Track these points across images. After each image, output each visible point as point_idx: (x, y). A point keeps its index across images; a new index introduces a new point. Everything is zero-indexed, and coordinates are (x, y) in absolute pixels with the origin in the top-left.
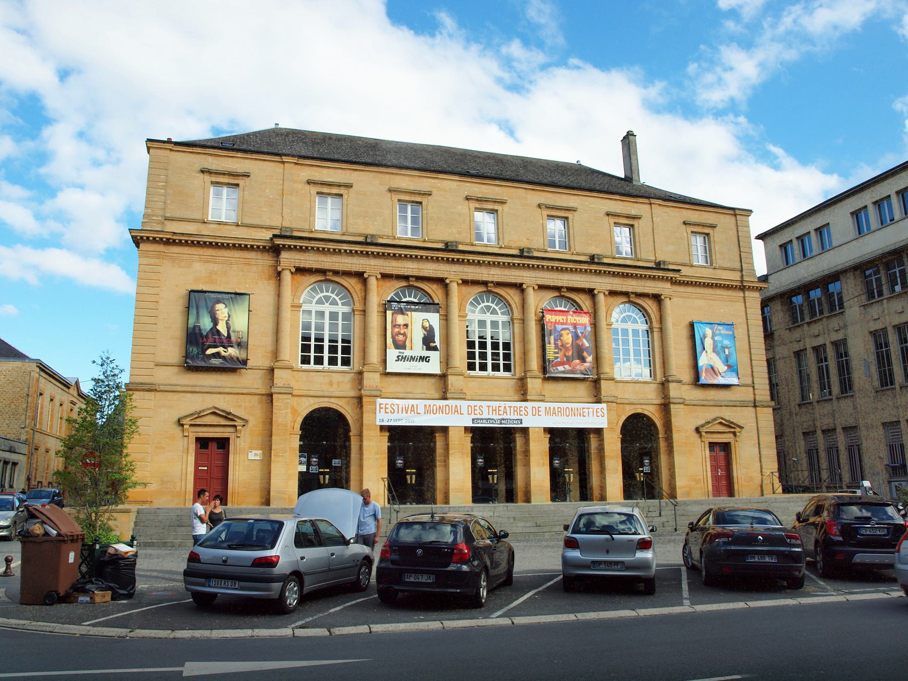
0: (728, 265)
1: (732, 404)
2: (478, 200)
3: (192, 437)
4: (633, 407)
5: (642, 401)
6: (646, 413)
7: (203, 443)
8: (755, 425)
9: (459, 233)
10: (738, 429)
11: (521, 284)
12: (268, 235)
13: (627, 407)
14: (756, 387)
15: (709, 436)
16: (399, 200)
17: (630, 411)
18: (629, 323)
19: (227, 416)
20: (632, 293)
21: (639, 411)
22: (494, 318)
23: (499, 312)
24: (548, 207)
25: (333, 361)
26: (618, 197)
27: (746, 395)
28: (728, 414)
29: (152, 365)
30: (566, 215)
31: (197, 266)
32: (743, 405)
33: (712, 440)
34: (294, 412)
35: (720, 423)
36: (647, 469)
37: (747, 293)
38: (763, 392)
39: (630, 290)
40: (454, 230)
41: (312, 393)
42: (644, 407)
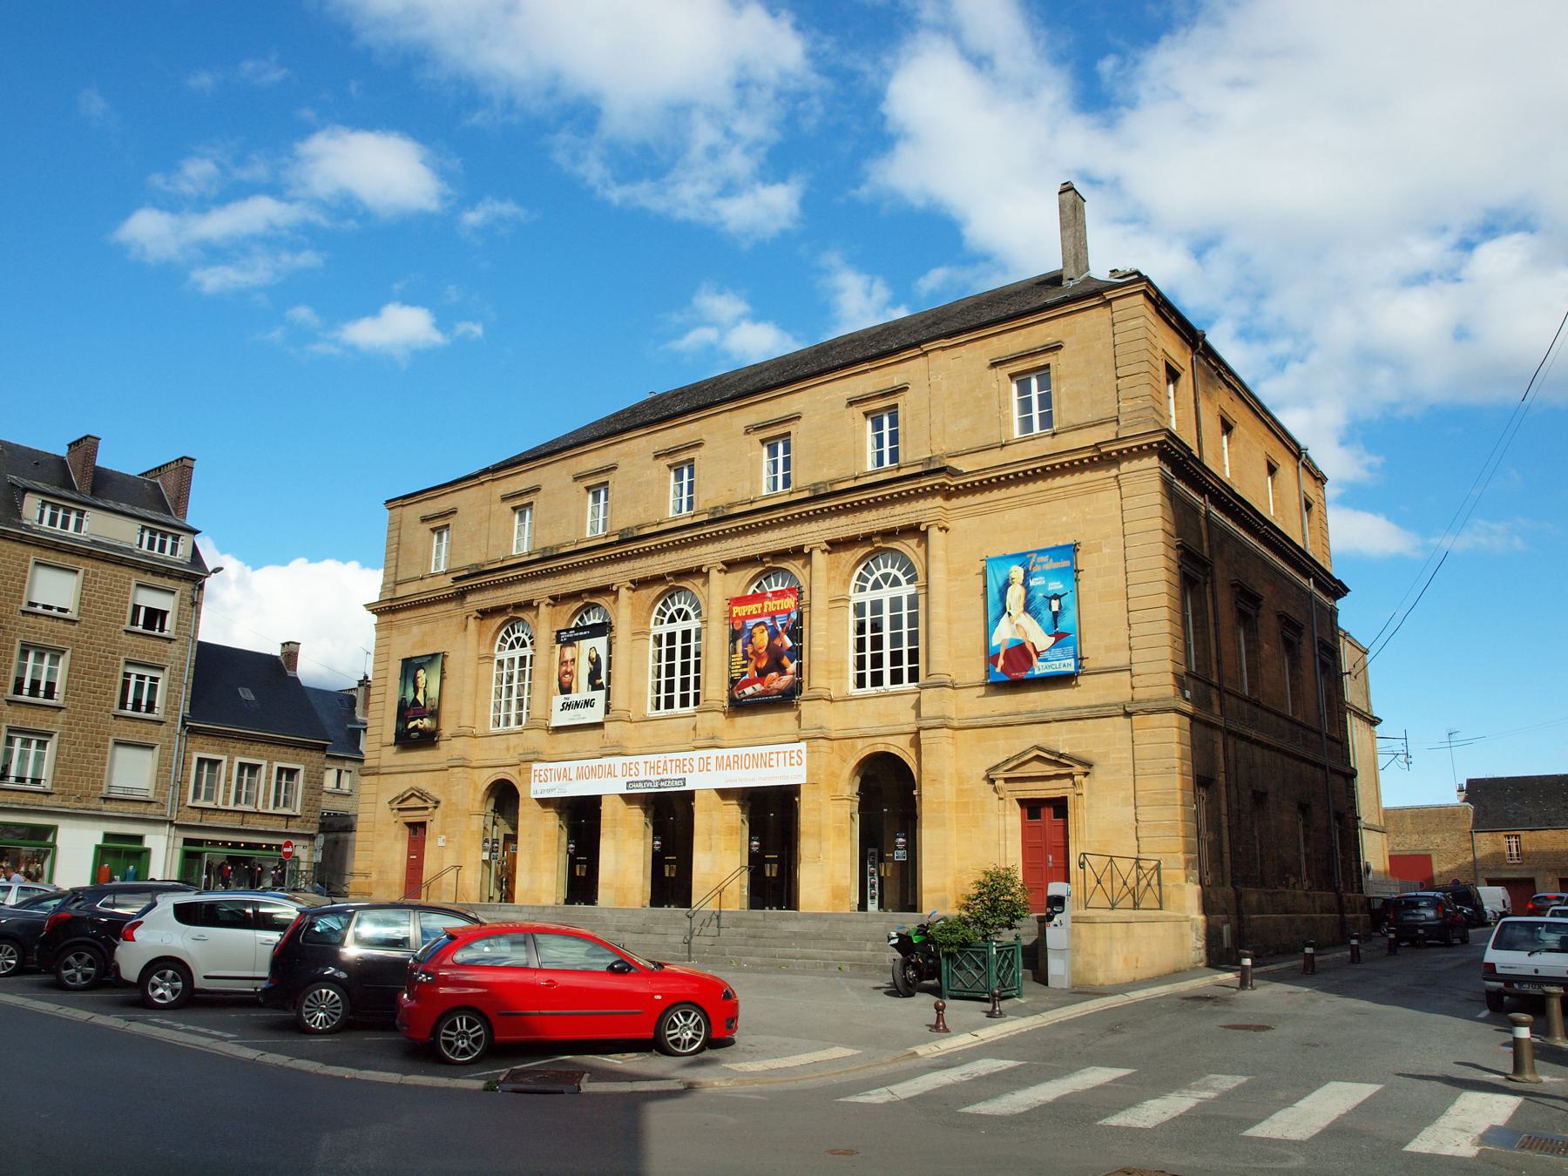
0: (1090, 417)
1: (1070, 714)
2: (669, 453)
3: (401, 821)
4: (870, 741)
5: (883, 730)
6: (893, 750)
7: (410, 825)
8: (1128, 755)
9: (645, 511)
10: (1078, 769)
11: (699, 569)
12: (448, 581)
13: (860, 743)
14: (1135, 669)
15: (1017, 786)
16: (763, 442)
17: (864, 749)
18: (886, 587)
19: (423, 796)
20: (669, 574)
21: (881, 748)
22: (686, 625)
23: (903, 579)
24: (758, 428)
25: (684, 702)
26: (866, 366)
27: (1114, 689)
28: (1062, 739)
29: (378, 746)
30: (786, 430)
31: (415, 629)
32: (1099, 713)
33: (1022, 795)
34: (476, 788)
35: (1038, 758)
36: (900, 855)
37: (1125, 466)
38: (1155, 680)
39: (862, 530)
40: (640, 509)
41: (488, 763)
42: (889, 740)
